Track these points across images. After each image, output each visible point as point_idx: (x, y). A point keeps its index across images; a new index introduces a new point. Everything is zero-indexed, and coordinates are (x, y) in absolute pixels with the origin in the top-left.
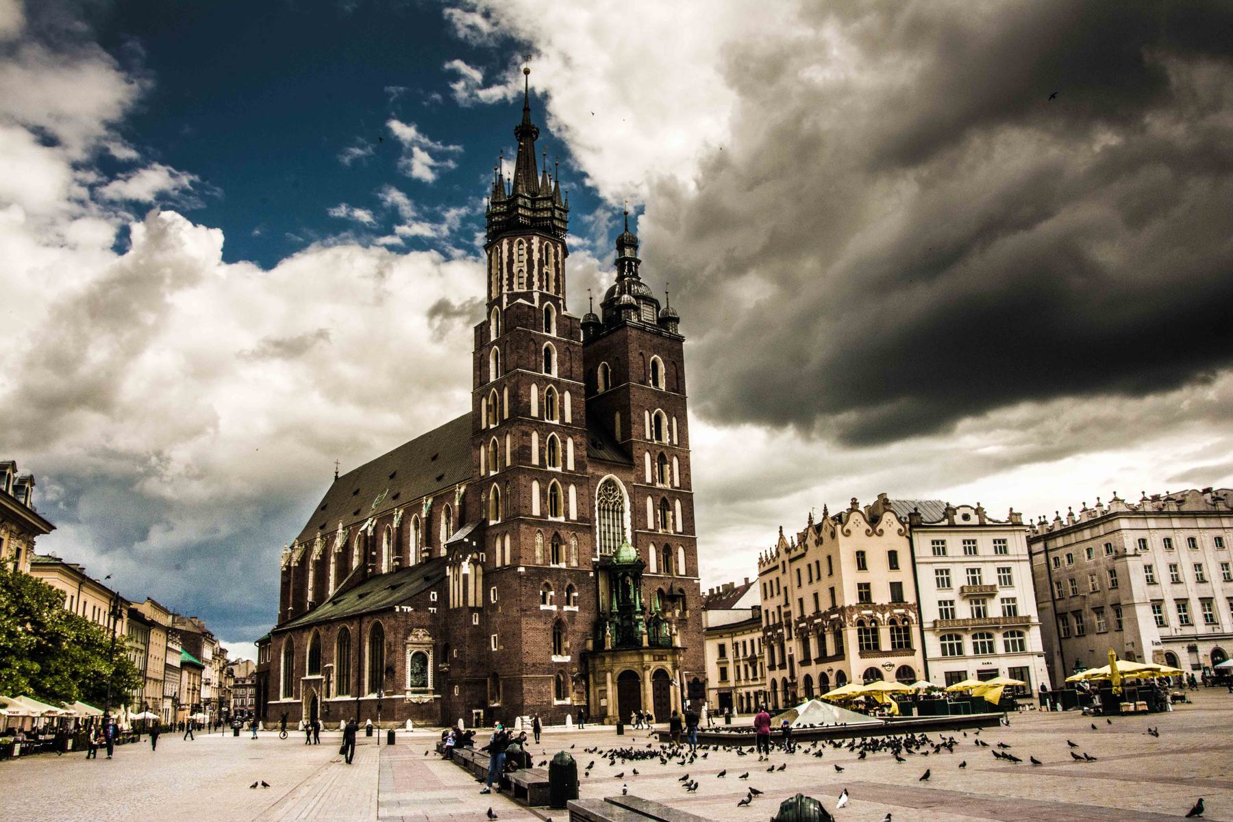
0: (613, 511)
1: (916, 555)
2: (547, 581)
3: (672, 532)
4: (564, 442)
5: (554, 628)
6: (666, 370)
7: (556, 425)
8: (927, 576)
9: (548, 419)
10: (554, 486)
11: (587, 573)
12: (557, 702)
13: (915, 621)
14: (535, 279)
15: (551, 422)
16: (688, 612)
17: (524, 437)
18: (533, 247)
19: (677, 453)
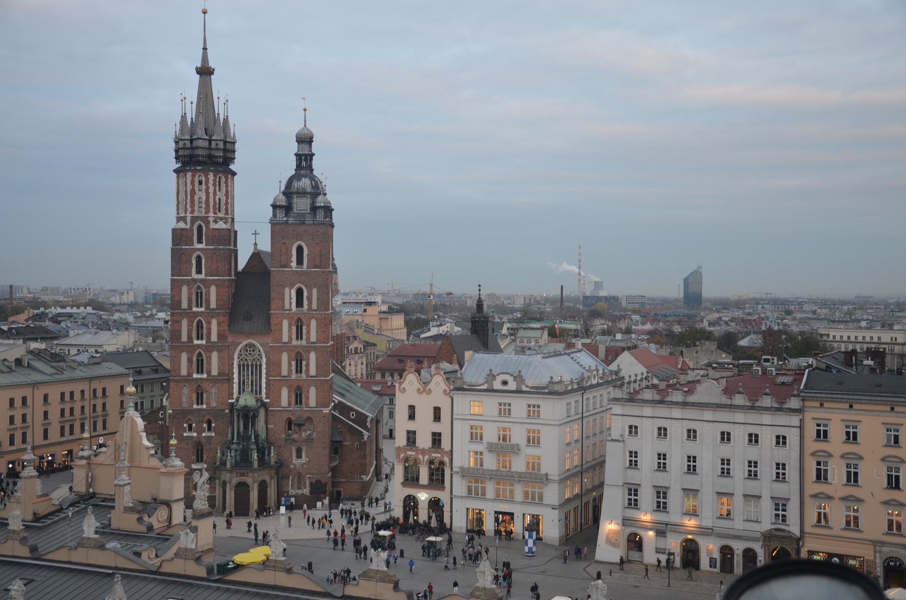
0: (252, 365)
2: (190, 417)
3: (304, 376)
4: (209, 323)
6: (309, 251)
7: (201, 312)
8: (462, 431)
9: (197, 306)
10: (200, 354)
11: (223, 410)
13: (448, 465)
14: (188, 206)
15: (200, 310)
16: (315, 433)
17: (175, 324)
18: (188, 181)
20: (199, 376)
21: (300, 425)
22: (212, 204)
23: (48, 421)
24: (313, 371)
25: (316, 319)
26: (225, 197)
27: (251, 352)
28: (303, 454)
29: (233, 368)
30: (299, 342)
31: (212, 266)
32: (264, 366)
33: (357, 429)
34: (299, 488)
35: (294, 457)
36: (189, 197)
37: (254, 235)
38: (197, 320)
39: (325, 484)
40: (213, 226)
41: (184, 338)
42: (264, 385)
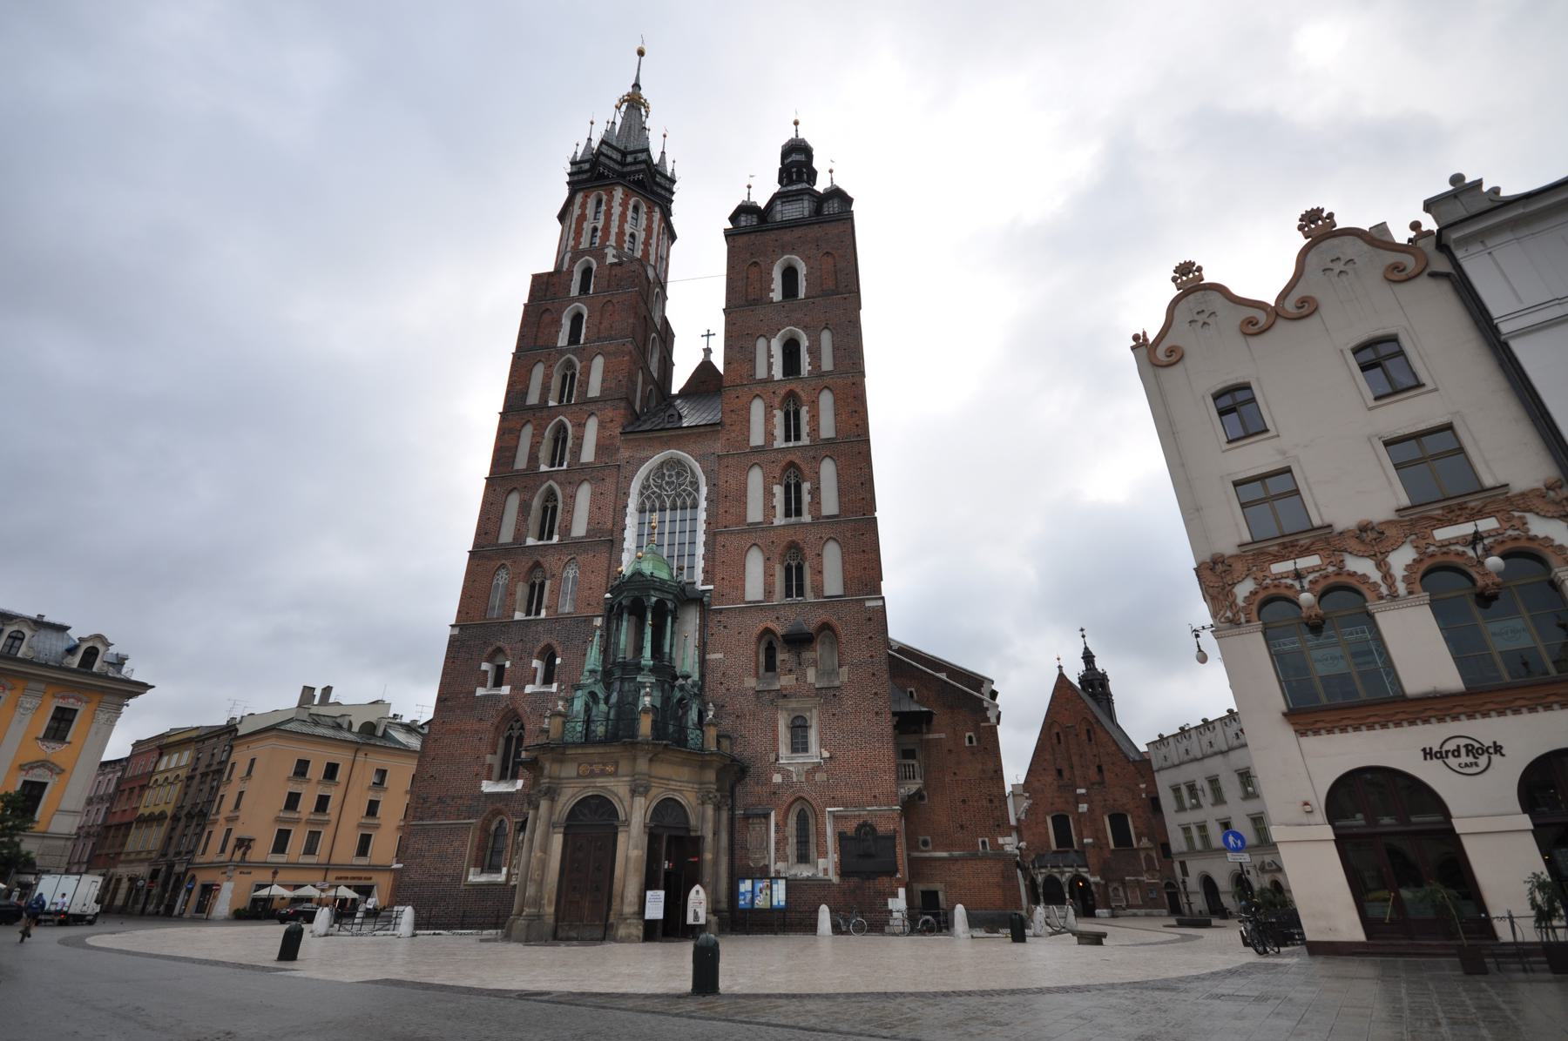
0: (674, 508)
1: (1495, 310)
2: (498, 644)
4: (581, 426)
5: (511, 728)
9: (561, 401)
12: (475, 877)
16: (845, 669)
17: (506, 436)
19: (827, 381)
20: (541, 543)
21: (799, 641)
22: (614, 230)
23: (376, 822)
24: (830, 505)
25: (831, 390)
26: (643, 235)
27: (674, 479)
28: (813, 736)
29: (626, 515)
30: (791, 444)
31: (601, 323)
32: (703, 504)
33: (962, 690)
34: (803, 858)
35: (784, 749)
36: (573, 226)
37: (706, 338)
38: (557, 419)
39: (891, 838)
40: (610, 260)
41: (521, 463)
42: (700, 550)
